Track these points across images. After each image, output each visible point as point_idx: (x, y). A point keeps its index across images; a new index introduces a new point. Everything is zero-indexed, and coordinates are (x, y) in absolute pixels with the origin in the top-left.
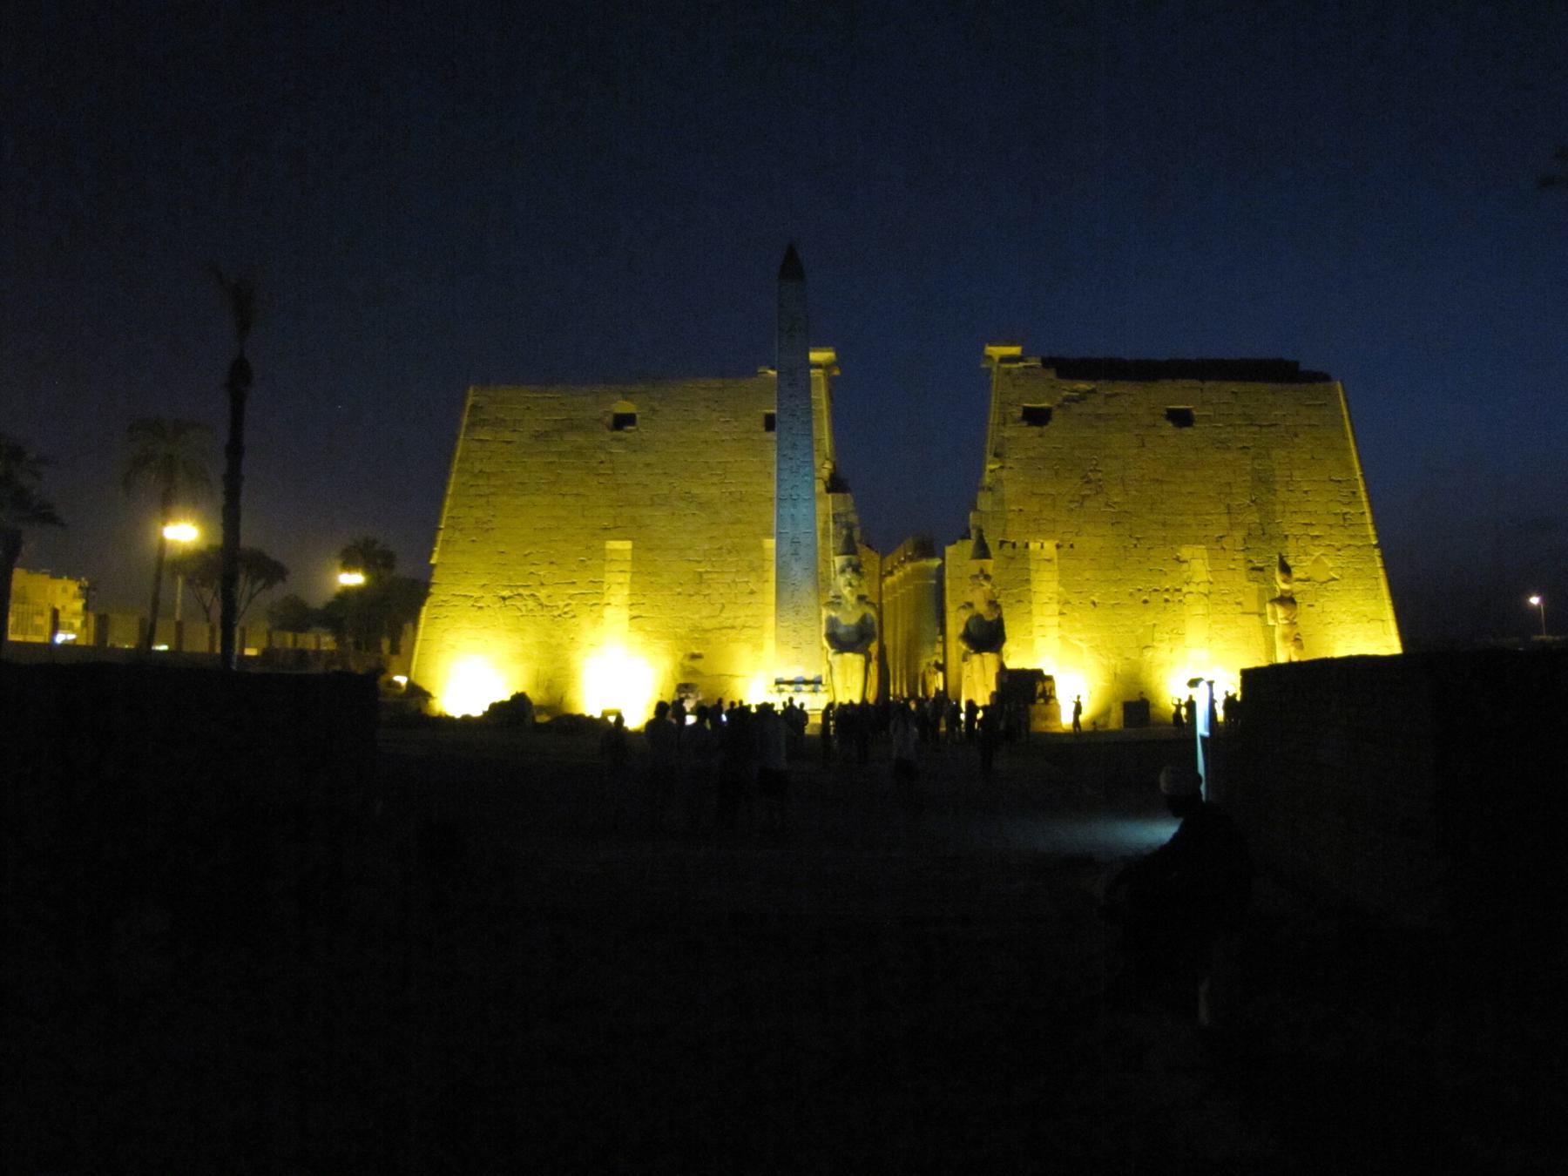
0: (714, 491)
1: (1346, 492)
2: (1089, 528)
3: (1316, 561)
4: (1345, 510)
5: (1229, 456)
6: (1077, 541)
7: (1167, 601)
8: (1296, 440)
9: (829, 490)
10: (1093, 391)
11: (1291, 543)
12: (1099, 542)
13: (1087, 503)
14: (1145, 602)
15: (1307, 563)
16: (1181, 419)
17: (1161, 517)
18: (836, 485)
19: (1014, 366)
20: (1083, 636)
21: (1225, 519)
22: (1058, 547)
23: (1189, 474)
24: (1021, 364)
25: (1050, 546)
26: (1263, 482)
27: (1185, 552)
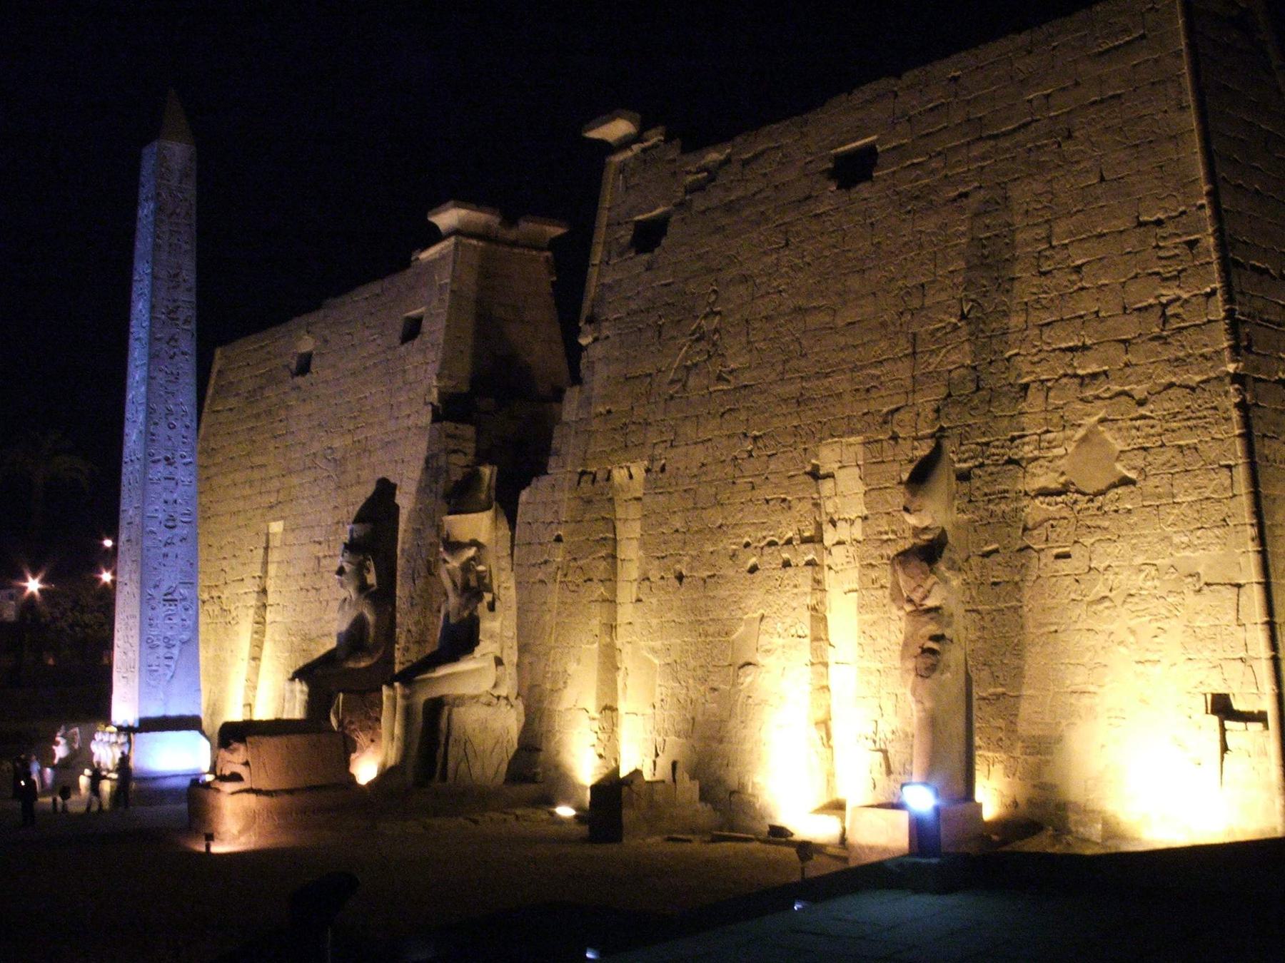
0: (348, 440)
1: (1171, 246)
2: (689, 430)
3: (1084, 439)
4: (1169, 293)
5: (929, 224)
6: (675, 458)
7: (787, 564)
8: (1068, 147)
9: (436, 418)
10: (728, 161)
11: (1035, 400)
12: (699, 454)
13: (692, 382)
14: (753, 569)
15: (1065, 448)
16: (853, 170)
17: (792, 389)
18: (449, 410)
19: (629, 154)
20: (658, 644)
21: (903, 371)
22: (648, 471)
23: (854, 282)
24: (636, 148)
25: (638, 470)
26: (990, 264)
27: (828, 457)
